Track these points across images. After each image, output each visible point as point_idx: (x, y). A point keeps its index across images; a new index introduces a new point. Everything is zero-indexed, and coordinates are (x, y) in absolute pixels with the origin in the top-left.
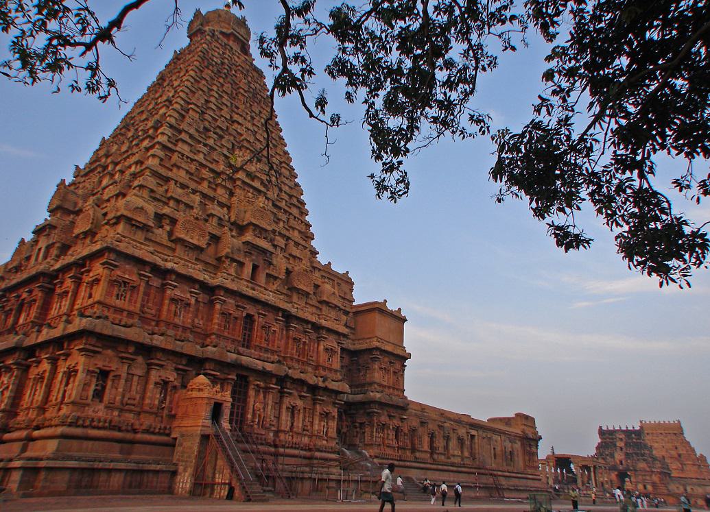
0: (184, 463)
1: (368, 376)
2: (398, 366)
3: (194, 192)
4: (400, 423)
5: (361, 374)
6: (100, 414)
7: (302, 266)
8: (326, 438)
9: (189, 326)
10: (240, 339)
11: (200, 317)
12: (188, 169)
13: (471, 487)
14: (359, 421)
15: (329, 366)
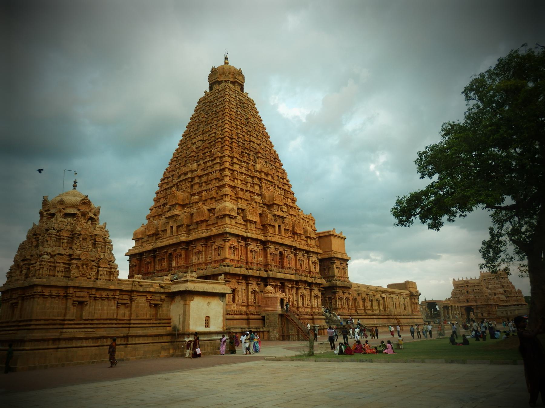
0: (272, 327)
1: (330, 272)
2: (344, 265)
3: (246, 191)
4: (348, 295)
5: (326, 271)
6: (235, 308)
7: (297, 220)
8: (317, 308)
9: (258, 262)
10: (279, 265)
11: (261, 257)
12: (241, 179)
13: (386, 326)
14: (327, 297)
15: (314, 271)
